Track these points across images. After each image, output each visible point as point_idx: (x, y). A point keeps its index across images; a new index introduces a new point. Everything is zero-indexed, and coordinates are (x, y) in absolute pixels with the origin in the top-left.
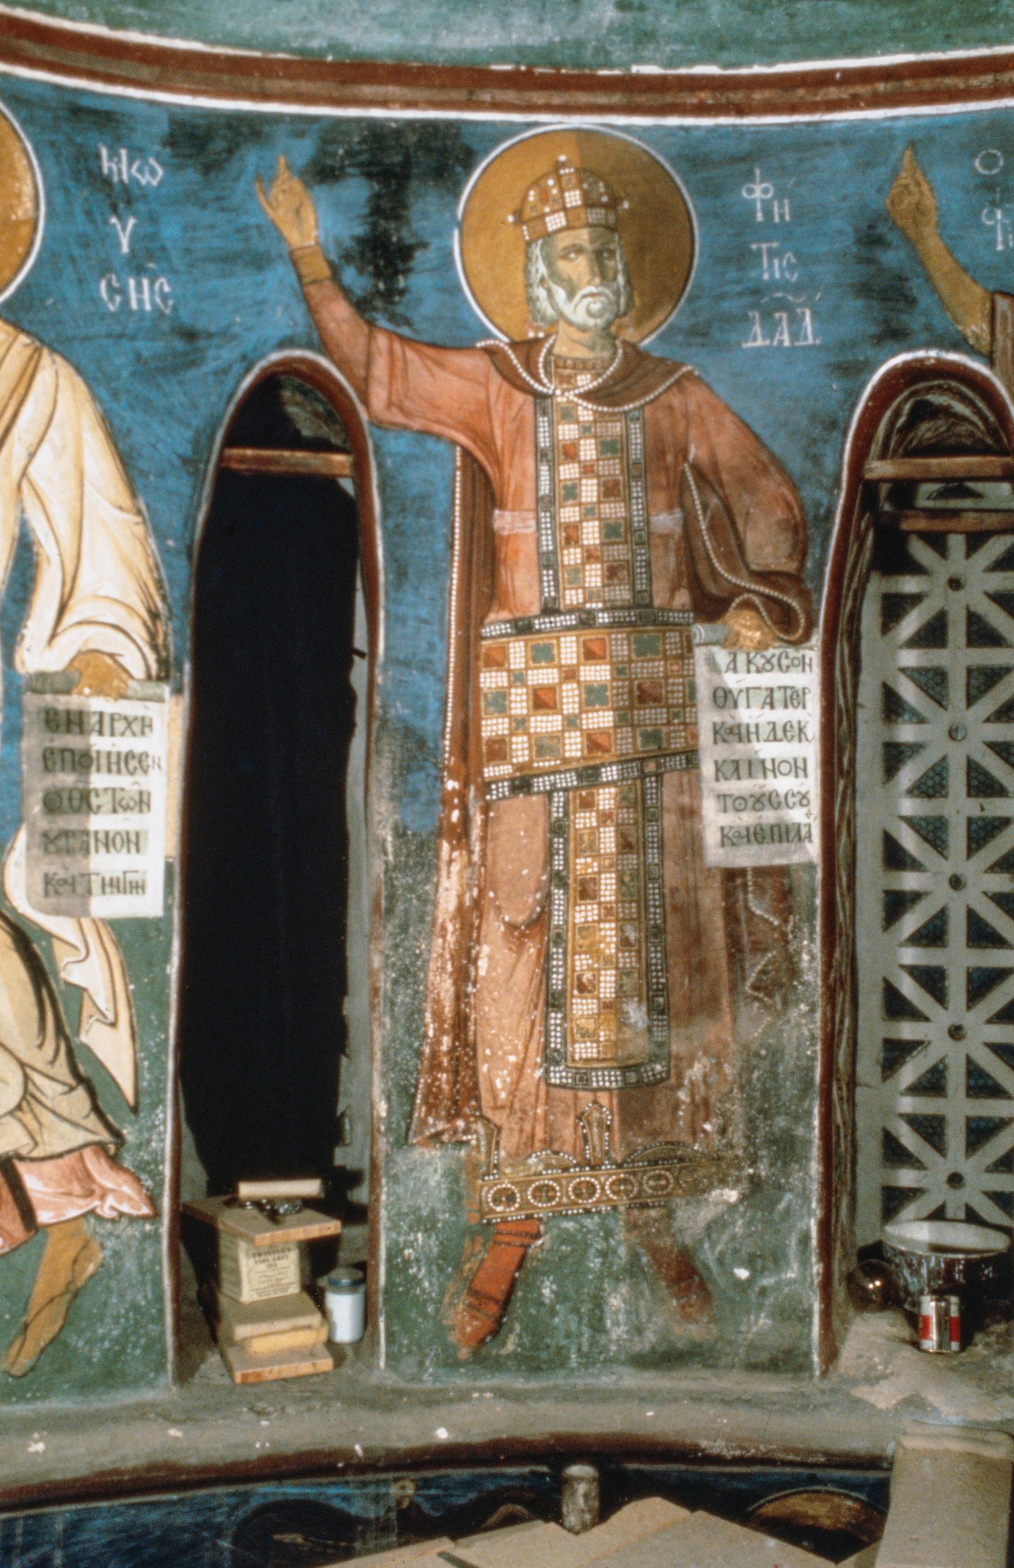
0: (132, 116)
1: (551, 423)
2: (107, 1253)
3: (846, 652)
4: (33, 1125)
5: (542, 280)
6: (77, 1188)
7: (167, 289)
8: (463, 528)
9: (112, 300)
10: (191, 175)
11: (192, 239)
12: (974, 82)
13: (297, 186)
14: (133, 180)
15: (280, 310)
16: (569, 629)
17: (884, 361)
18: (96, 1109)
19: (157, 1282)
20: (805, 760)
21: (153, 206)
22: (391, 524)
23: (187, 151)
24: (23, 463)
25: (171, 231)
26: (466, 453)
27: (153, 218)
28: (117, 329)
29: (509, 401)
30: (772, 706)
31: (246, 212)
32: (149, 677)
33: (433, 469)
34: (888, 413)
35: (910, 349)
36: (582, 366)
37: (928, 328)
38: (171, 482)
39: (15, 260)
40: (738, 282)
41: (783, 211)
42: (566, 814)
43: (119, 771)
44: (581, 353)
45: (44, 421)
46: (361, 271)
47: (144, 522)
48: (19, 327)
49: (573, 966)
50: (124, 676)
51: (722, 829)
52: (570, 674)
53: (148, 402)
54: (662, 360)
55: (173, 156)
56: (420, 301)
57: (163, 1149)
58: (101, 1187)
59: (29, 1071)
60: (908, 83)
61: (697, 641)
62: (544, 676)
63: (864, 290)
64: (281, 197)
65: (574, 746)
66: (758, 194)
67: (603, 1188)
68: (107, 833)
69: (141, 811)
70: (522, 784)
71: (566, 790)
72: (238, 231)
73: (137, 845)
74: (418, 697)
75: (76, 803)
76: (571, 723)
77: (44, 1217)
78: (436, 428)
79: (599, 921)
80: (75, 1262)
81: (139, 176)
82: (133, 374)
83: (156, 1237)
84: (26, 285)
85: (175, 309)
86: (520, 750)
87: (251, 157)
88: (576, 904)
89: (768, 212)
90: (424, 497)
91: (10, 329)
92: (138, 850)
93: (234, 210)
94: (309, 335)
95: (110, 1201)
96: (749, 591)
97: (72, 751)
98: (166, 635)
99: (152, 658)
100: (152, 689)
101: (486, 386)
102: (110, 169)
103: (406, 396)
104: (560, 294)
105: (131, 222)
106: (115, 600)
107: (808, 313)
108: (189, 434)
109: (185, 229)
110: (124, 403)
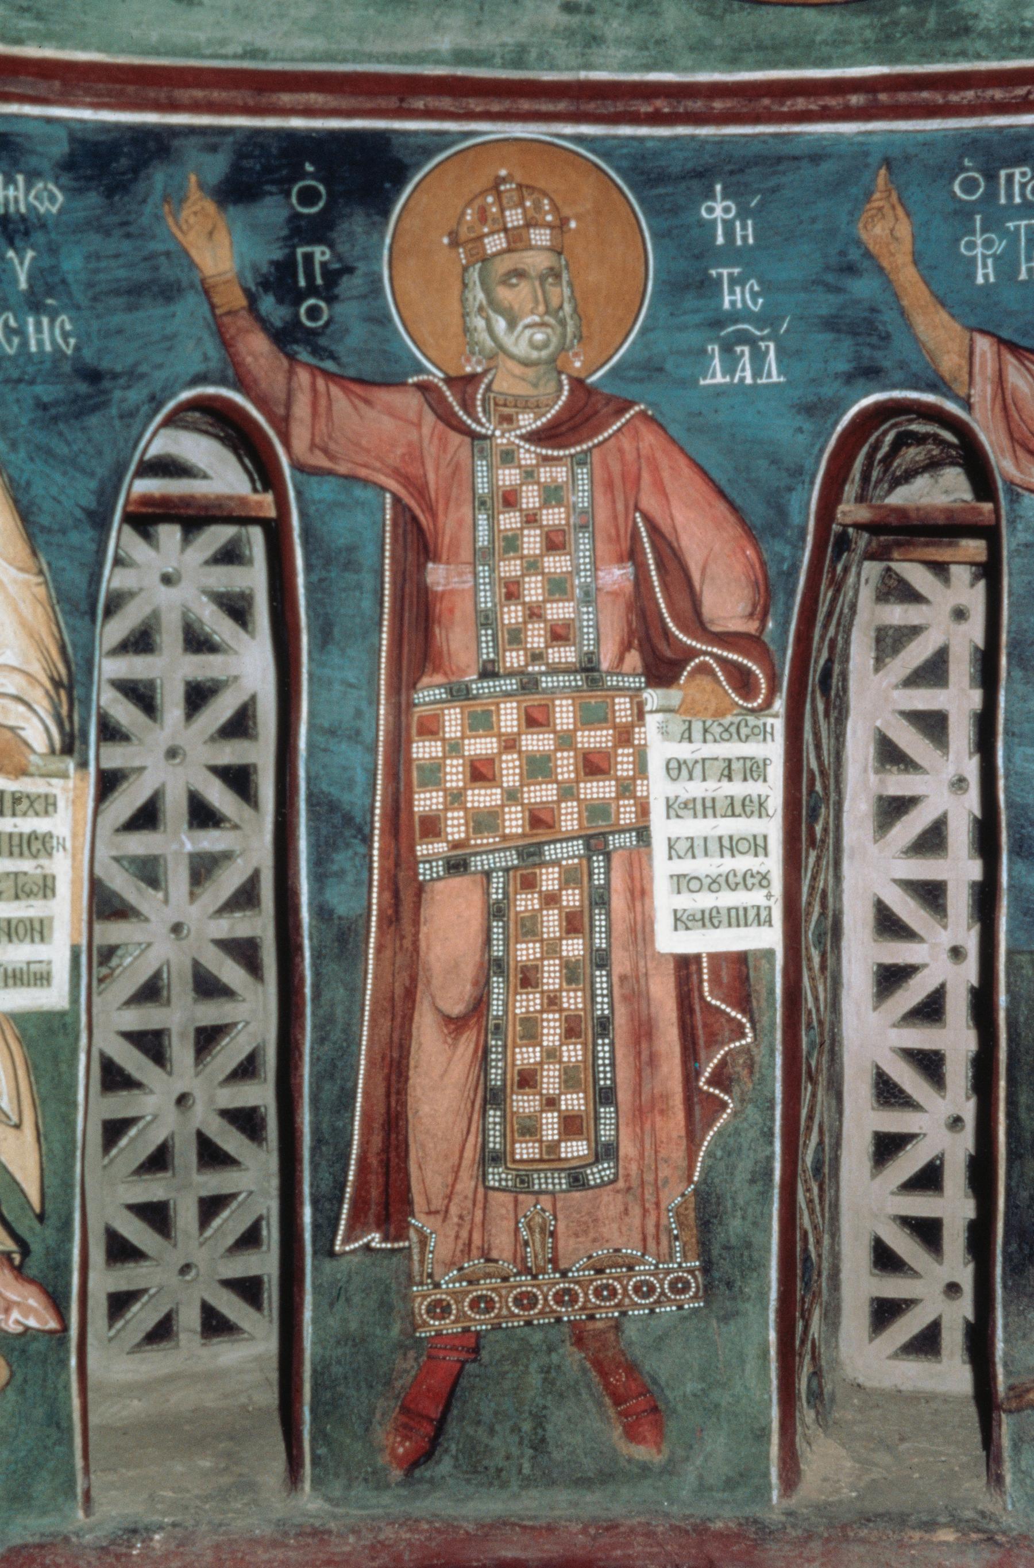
0: (28, 137)
1: (490, 467)
3: (821, 707)
5: (481, 309)
7: (68, 327)
8: (394, 583)
10: (93, 198)
11: (96, 271)
12: (954, 98)
13: (210, 207)
14: (31, 208)
15: (191, 344)
16: (508, 695)
17: (856, 402)
20: (765, 837)
21: (53, 236)
22: (315, 578)
23: (89, 172)
25: (72, 263)
26: (397, 500)
27: (53, 250)
28: (15, 374)
29: (443, 444)
30: (730, 779)
31: (153, 237)
32: (53, 752)
33: (360, 518)
34: (865, 449)
35: (884, 388)
36: (525, 404)
37: (902, 365)
38: (75, 537)
40: (697, 311)
41: (746, 233)
42: (506, 894)
43: (21, 854)
44: (522, 389)
46: (280, 301)
47: (46, 583)
49: (514, 1060)
51: (675, 911)
52: (510, 744)
53: (49, 453)
54: (609, 399)
56: (347, 331)
60: (883, 97)
61: (648, 708)
62: (482, 746)
63: (831, 324)
64: (192, 220)
65: (514, 822)
66: (718, 213)
67: (546, 1299)
69: (45, 896)
70: (456, 866)
71: (506, 870)
72: (145, 259)
73: (41, 933)
74: (345, 769)
76: (512, 796)
78: (363, 472)
79: (542, 1012)
81: (37, 204)
82: (32, 422)
85: (77, 348)
86: (455, 827)
87: (159, 177)
88: (516, 993)
89: (730, 233)
90: (351, 549)
92: (42, 939)
93: (141, 235)
94: (223, 371)
95: (15, 1315)
96: (706, 653)
101: (419, 426)
103: (330, 437)
104: (501, 324)
105: (30, 254)
106: (14, 669)
107: (772, 346)
108: (93, 485)
109: (88, 258)
110: (22, 454)
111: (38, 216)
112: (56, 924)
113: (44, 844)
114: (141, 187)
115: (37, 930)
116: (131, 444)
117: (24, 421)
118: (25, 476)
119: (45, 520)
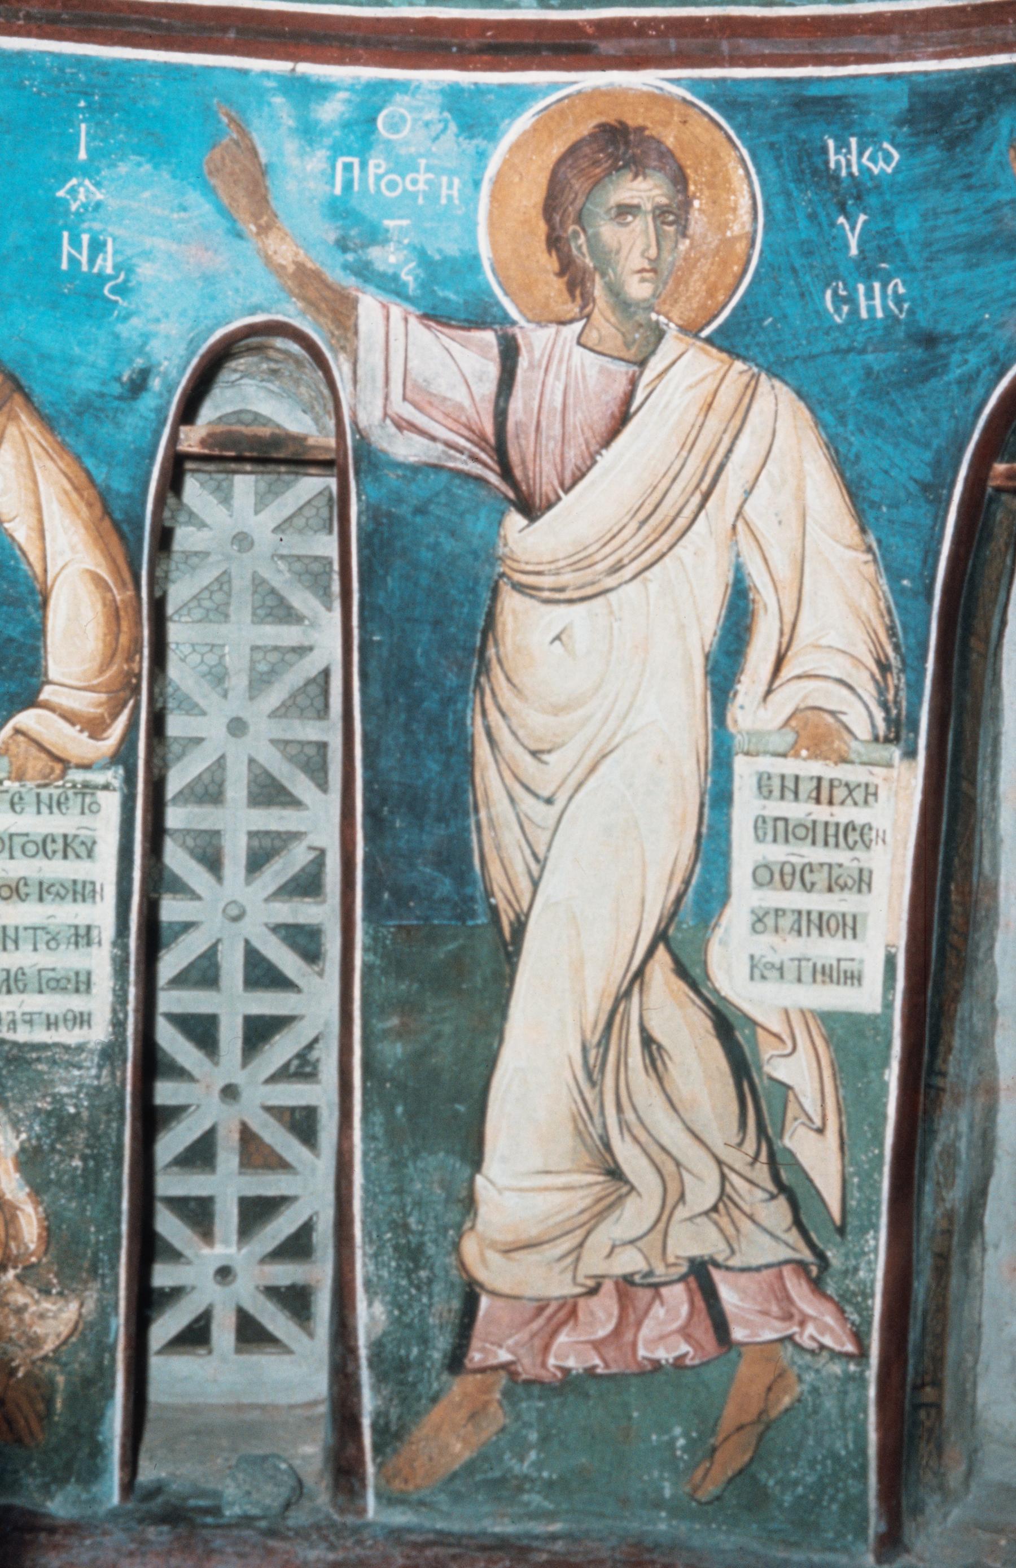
2: (805, 1387)
4: (730, 1230)
6: (775, 1309)
7: (901, 290)
9: (838, 310)
10: (932, 153)
14: (864, 170)
18: (798, 1223)
19: (861, 1435)
21: (888, 197)
23: (929, 126)
24: (738, 503)
25: (908, 224)
27: (887, 212)
28: (844, 344)
31: (996, 186)
32: (876, 739)
39: (729, 280)
45: (763, 453)
47: (875, 560)
48: (734, 354)
50: (847, 736)
53: (880, 423)
55: (911, 135)
57: (873, 1282)
58: (801, 1312)
59: (726, 1170)
68: (821, 915)
69: (860, 891)
72: (987, 212)
73: (854, 929)
75: (788, 879)
77: (738, 1334)
80: (769, 1389)
81: (870, 165)
82: (862, 393)
83: (861, 1381)
84: (742, 306)
85: (911, 312)
91: (724, 356)
92: (855, 936)
93: (983, 186)
95: (810, 1329)
97: (786, 820)
98: (897, 688)
99: (879, 715)
100: (882, 752)
102: (838, 163)
105: (862, 218)
106: (844, 652)
108: (928, 456)
109: (925, 217)
110: (851, 427)
111: (872, 177)
112: (870, 921)
113: (862, 835)
114: (985, 135)
115: (849, 926)
116: (972, 409)
117: (853, 393)
118: (854, 450)
119: (874, 495)
